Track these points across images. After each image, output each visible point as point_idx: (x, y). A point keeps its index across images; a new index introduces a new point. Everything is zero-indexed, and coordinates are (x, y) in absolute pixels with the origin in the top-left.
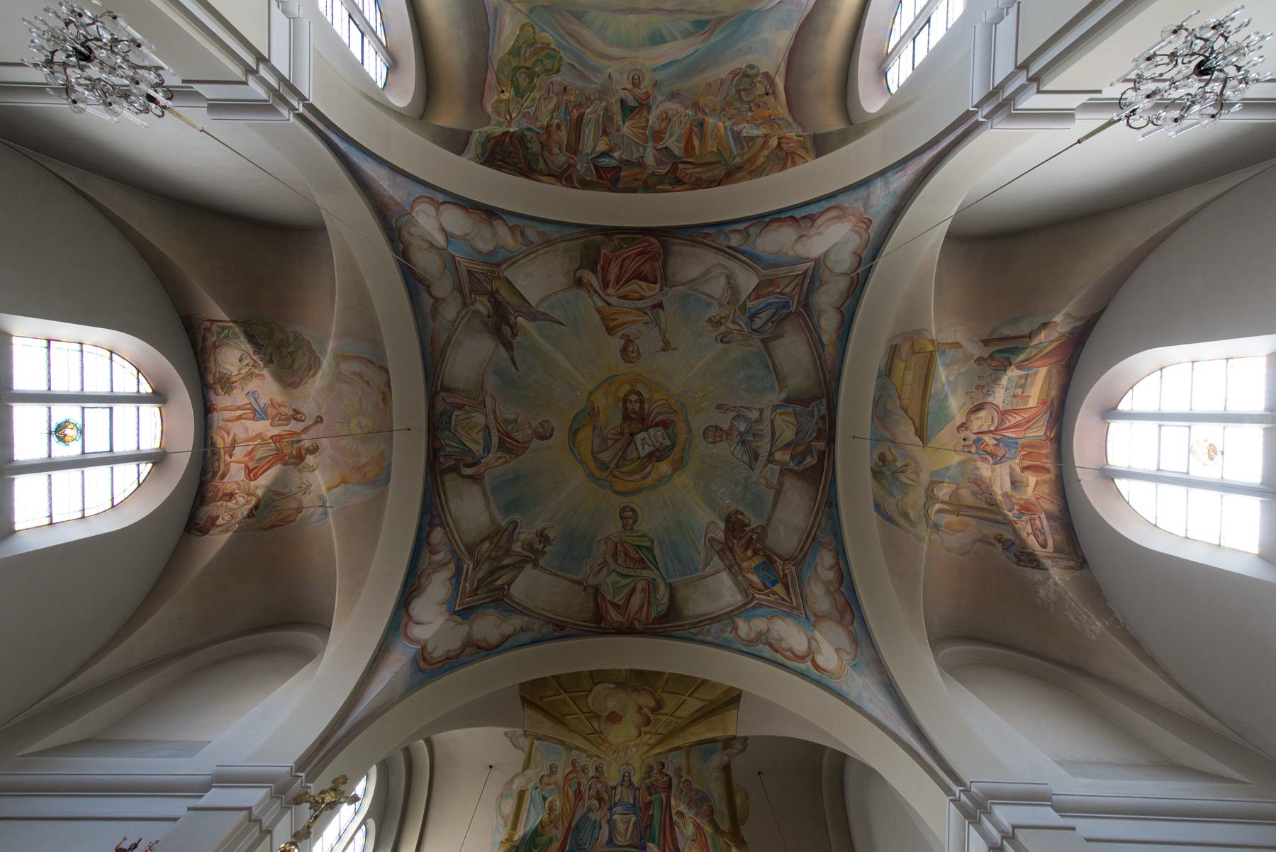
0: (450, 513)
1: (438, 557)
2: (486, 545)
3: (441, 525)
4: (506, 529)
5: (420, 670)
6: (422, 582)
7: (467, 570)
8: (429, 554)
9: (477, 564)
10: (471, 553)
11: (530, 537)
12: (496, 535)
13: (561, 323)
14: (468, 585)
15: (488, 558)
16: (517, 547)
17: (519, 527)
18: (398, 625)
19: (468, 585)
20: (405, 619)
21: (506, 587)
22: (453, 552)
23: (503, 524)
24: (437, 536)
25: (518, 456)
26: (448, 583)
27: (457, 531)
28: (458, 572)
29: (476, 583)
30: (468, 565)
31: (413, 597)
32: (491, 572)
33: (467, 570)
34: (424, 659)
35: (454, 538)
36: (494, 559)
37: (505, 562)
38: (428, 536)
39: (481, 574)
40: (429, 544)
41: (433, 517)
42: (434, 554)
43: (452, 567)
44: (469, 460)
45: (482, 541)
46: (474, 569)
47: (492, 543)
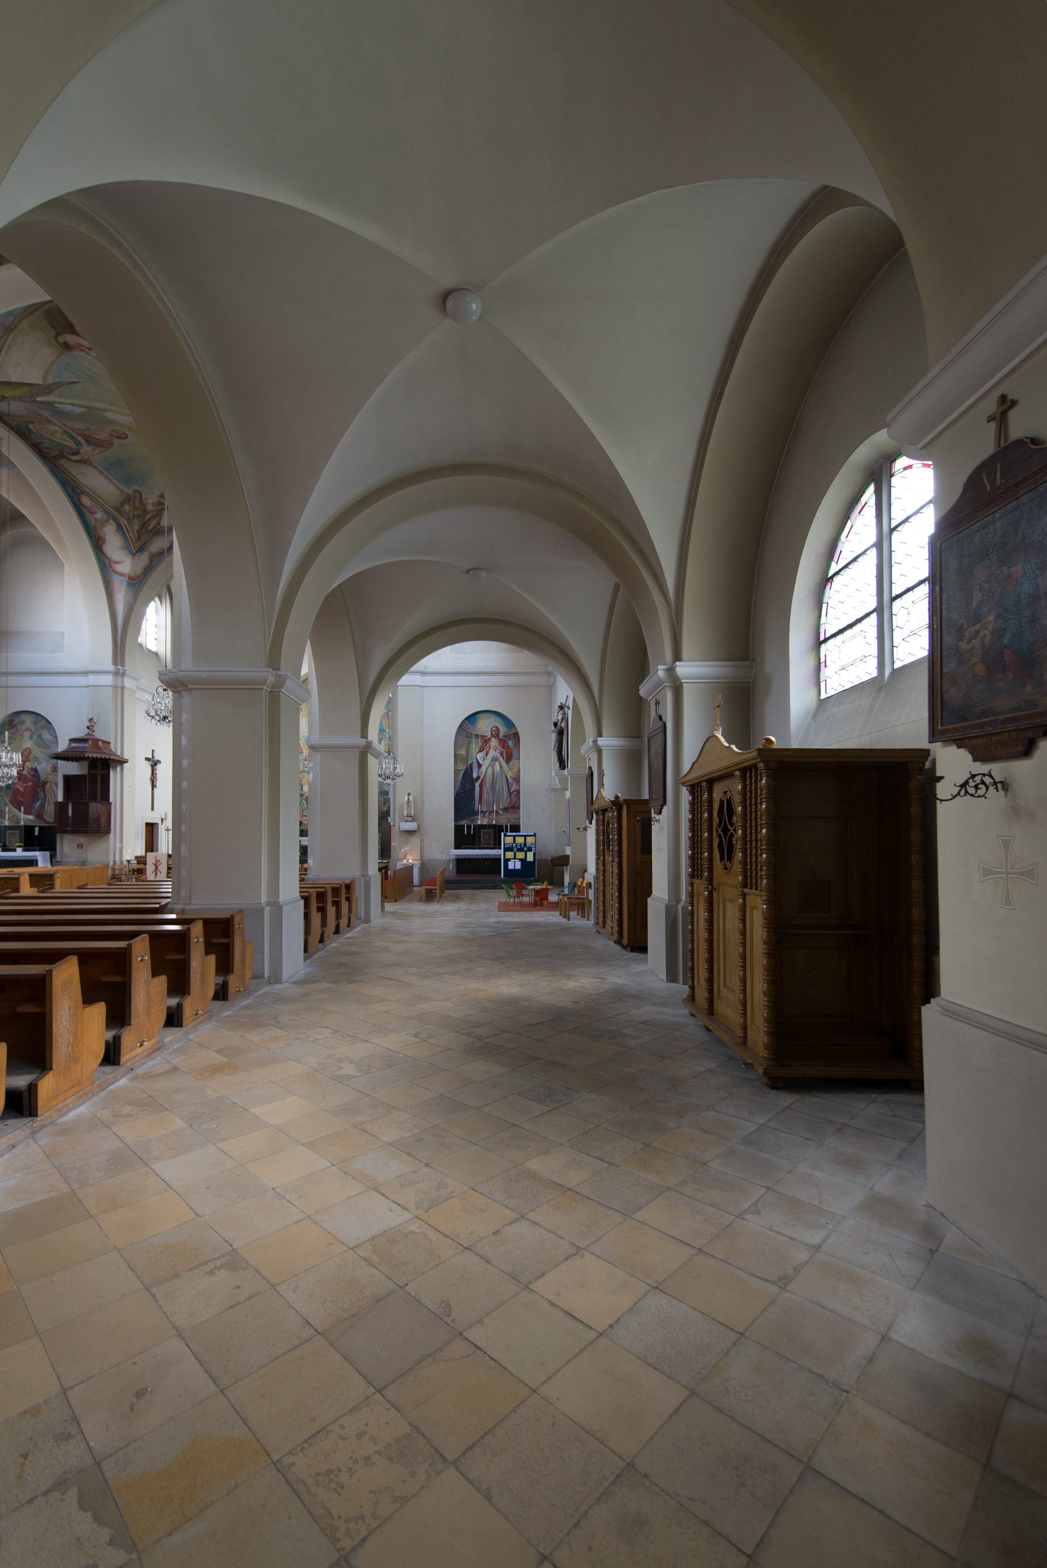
0: (84, 485)
1: (99, 515)
2: (127, 507)
3: (83, 493)
4: (134, 496)
5: (134, 584)
6: (100, 533)
7: (125, 525)
8: (91, 514)
9: (129, 520)
10: (120, 513)
11: (155, 500)
12: (130, 500)
13: (77, 382)
14: (131, 535)
15: (134, 516)
16: (150, 507)
17: (143, 494)
18: (106, 567)
19: (131, 535)
20: (106, 560)
21: (158, 526)
22: (106, 512)
23: (130, 492)
24: (86, 501)
25: (108, 448)
26: (117, 534)
27: (100, 498)
28: (119, 527)
29: (136, 533)
30: (123, 522)
31: (101, 545)
32: (143, 525)
33: (125, 525)
34: (133, 580)
35: (99, 502)
36: (138, 516)
37: (147, 517)
38: (80, 501)
39: (136, 528)
40: (85, 507)
41: (72, 488)
42: (94, 513)
43: (111, 521)
44: (70, 451)
45: (122, 504)
46: (129, 524)
47: (130, 505)
